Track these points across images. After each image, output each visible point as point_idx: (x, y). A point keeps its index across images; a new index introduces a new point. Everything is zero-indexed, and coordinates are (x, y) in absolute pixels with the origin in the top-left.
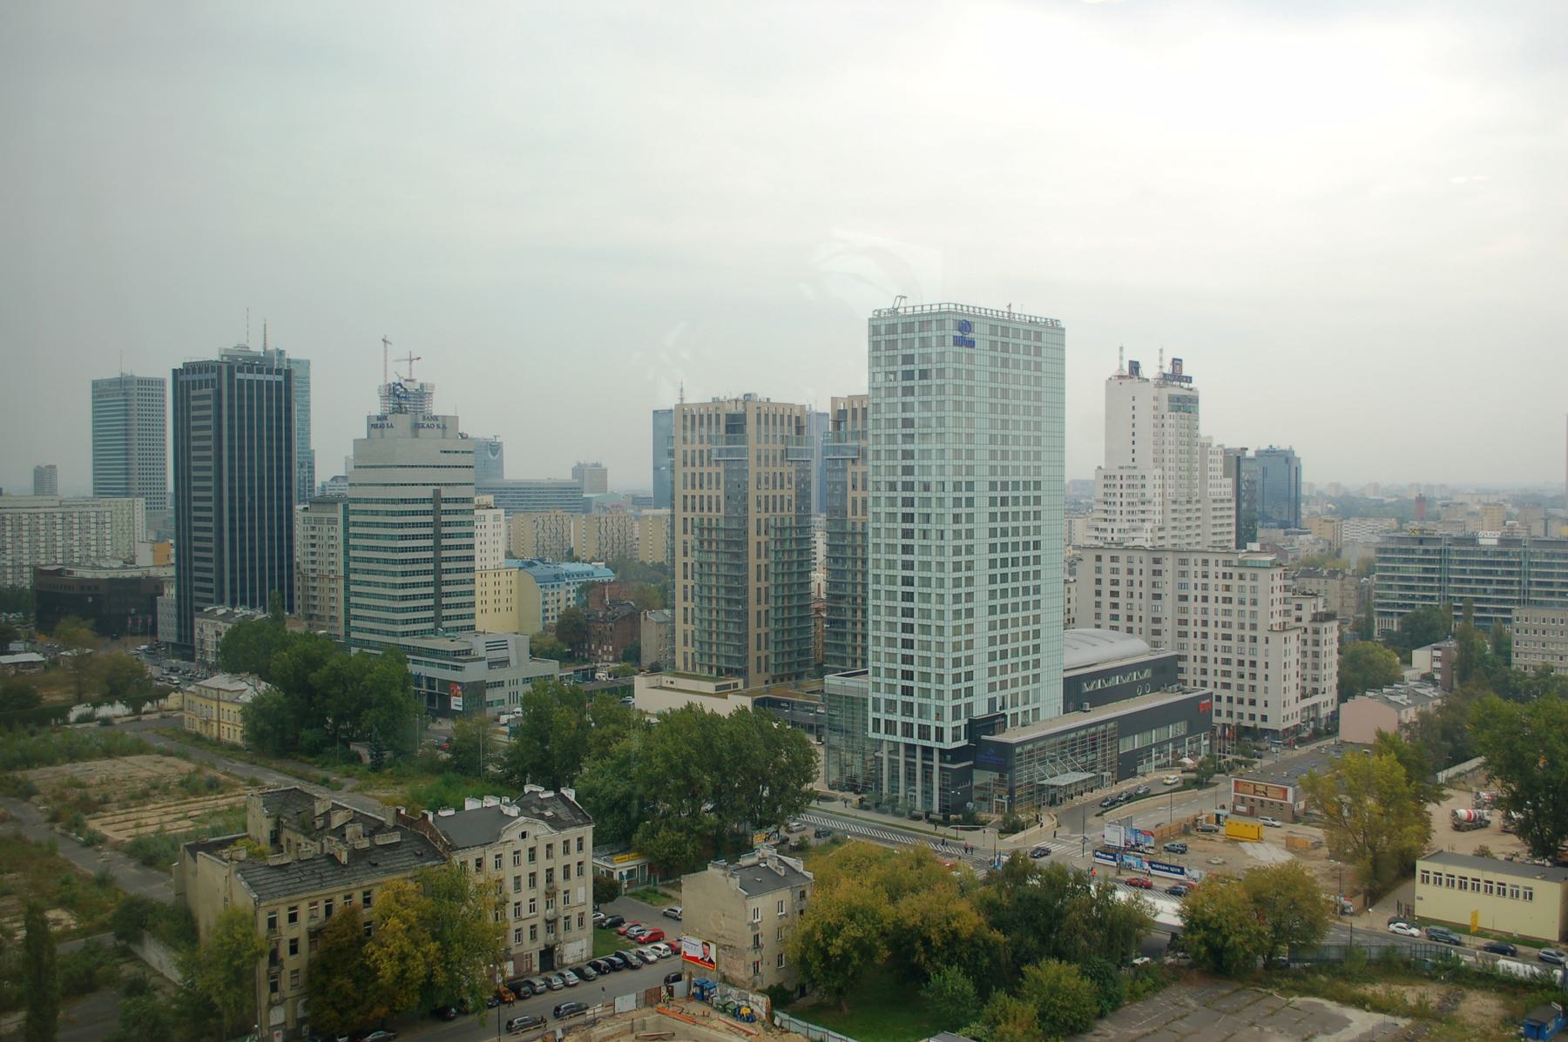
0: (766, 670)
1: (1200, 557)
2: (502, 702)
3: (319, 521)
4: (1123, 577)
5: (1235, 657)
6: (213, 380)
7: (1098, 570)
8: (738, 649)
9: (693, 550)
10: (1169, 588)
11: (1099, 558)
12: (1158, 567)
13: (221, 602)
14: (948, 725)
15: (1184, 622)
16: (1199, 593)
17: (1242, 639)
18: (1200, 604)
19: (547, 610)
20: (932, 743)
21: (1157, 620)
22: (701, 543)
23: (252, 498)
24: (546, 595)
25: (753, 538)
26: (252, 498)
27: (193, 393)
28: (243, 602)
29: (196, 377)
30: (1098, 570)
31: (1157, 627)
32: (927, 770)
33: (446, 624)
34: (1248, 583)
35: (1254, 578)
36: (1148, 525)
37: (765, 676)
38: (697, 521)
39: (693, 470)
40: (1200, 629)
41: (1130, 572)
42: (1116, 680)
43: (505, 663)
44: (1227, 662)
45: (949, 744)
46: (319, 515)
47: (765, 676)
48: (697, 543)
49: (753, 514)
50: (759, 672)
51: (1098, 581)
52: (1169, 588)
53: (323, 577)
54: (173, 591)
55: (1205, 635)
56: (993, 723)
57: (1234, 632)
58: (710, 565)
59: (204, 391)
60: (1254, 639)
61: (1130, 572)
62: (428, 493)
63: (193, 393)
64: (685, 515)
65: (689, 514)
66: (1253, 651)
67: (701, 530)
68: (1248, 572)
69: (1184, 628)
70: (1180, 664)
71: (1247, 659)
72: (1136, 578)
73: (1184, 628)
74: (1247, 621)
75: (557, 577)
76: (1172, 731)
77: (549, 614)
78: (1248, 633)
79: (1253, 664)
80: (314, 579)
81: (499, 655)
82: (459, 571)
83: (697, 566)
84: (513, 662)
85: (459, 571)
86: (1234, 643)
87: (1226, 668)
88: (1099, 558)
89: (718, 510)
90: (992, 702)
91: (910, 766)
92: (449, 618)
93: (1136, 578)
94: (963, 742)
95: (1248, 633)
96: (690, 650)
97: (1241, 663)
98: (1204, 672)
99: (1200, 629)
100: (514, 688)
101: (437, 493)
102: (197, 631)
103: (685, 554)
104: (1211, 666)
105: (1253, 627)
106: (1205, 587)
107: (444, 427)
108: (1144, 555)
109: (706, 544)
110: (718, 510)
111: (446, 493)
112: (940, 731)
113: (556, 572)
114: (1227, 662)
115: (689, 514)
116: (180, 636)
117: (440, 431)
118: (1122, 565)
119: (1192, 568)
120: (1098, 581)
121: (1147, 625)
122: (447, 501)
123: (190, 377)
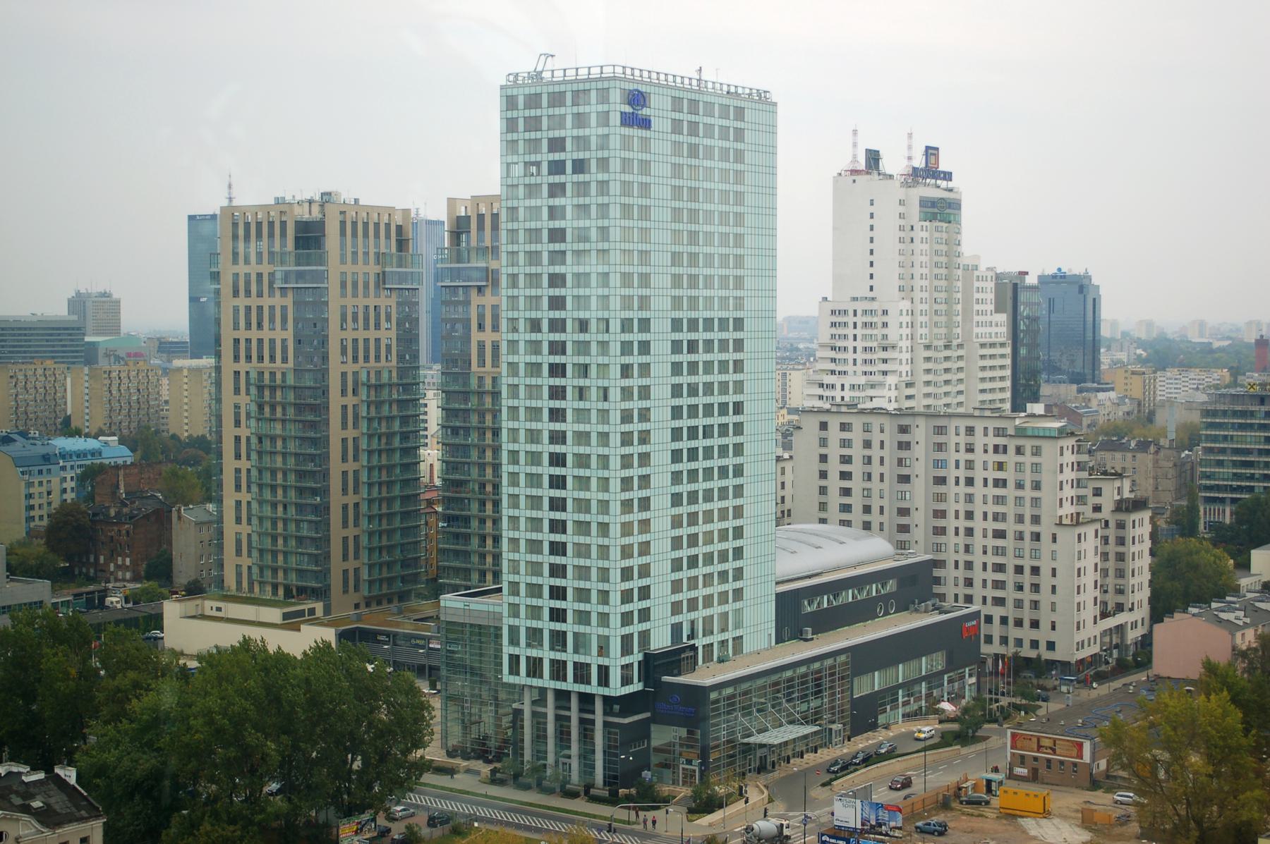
0: (357, 588)
1: (963, 424)
4: (857, 452)
5: (1010, 562)
7: (823, 442)
8: (315, 559)
9: (248, 416)
10: (920, 469)
11: (824, 426)
12: (905, 438)
14: (616, 662)
15: (941, 514)
16: (962, 473)
17: (1020, 536)
18: (963, 489)
19: (32, 507)
20: (593, 688)
21: (904, 512)
22: (261, 407)
24: (30, 484)
25: (336, 401)
30: (823, 442)
31: (904, 521)
32: (587, 727)
34: (1028, 459)
35: (1037, 452)
36: (891, 380)
37: (354, 597)
38: (253, 375)
39: (248, 302)
40: (963, 523)
41: (867, 444)
42: (849, 596)
44: (1000, 568)
45: (616, 688)
47: (354, 597)
48: (254, 408)
49: (336, 366)
50: (346, 591)
51: (824, 458)
52: (920, 469)
55: (970, 532)
56: (680, 657)
57: (1010, 527)
58: (273, 439)
60: (1036, 537)
61: (867, 444)
64: (237, 367)
65: (243, 366)
66: (1035, 554)
67: (261, 388)
68: (1028, 444)
69: (941, 523)
70: (937, 572)
71: (1027, 563)
72: (875, 453)
73: (941, 523)
74: (1028, 512)
75: (46, 458)
76: (925, 665)
77: (36, 513)
78: (1028, 528)
79: (1035, 571)
83: (254, 440)
86: (1009, 543)
87: (999, 577)
88: (824, 426)
89: (285, 360)
90: (676, 629)
91: (562, 721)
93: (875, 453)
94: (636, 687)
95: (1028, 528)
96: (245, 561)
97: (1019, 570)
98: (969, 583)
99: (963, 523)
103: (237, 423)
104: (978, 575)
105: (1036, 519)
106: (970, 465)
108: (886, 421)
109: (267, 409)
110: (285, 360)
112: (604, 672)
113: (43, 451)
114: (1000, 568)
115: (243, 366)
118: (856, 436)
119: (952, 439)
120: (824, 458)
121: (890, 519)
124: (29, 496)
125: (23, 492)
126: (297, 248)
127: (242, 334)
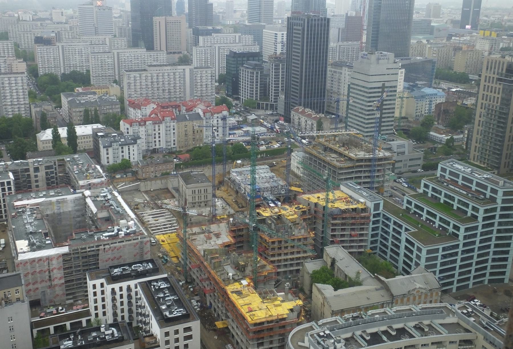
0: (508, 167)
2: (401, 167)
3: (335, 72)
6: (302, 24)
9: (484, 116)
13: (300, 105)
19: (417, 109)
22: (488, 114)
23: (313, 68)
24: (418, 103)
26: (313, 68)
27: (294, 27)
28: (307, 107)
29: (296, 21)
33: (382, 132)
38: (487, 105)
39: (489, 84)
43: (403, 153)
46: (336, 70)
48: (486, 114)
50: (505, 167)
53: (335, 93)
54: (284, 97)
58: (490, 124)
59: (298, 28)
62: (380, 85)
63: (294, 27)
64: (483, 101)
65: (484, 102)
67: (489, 109)
75: (423, 97)
77: (418, 111)
80: (331, 93)
81: (402, 150)
82: (389, 113)
83: (484, 123)
84: (406, 153)
85: (389, 113)
89: (497, 103)
92: (383, 130)
100: (405, 163)
101: (384, 84)
102: (292, 115)
103: (480, 117)
107: (389, 59)
109: (490, 115)
110: (497, 103)
111: (387, 84)
115: (484, 102)
116: (285, 113)
117: (387, 60)
122: (387, 87)
123: (294, 21)
124: (417, 107)
125: (415, 109)
126: (506, 72)
127: (486, 93)
